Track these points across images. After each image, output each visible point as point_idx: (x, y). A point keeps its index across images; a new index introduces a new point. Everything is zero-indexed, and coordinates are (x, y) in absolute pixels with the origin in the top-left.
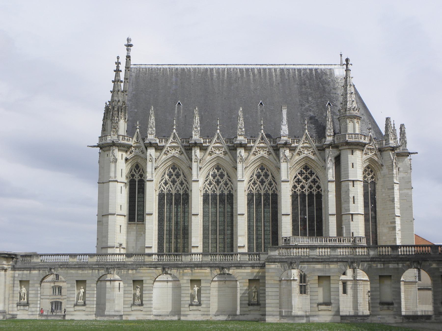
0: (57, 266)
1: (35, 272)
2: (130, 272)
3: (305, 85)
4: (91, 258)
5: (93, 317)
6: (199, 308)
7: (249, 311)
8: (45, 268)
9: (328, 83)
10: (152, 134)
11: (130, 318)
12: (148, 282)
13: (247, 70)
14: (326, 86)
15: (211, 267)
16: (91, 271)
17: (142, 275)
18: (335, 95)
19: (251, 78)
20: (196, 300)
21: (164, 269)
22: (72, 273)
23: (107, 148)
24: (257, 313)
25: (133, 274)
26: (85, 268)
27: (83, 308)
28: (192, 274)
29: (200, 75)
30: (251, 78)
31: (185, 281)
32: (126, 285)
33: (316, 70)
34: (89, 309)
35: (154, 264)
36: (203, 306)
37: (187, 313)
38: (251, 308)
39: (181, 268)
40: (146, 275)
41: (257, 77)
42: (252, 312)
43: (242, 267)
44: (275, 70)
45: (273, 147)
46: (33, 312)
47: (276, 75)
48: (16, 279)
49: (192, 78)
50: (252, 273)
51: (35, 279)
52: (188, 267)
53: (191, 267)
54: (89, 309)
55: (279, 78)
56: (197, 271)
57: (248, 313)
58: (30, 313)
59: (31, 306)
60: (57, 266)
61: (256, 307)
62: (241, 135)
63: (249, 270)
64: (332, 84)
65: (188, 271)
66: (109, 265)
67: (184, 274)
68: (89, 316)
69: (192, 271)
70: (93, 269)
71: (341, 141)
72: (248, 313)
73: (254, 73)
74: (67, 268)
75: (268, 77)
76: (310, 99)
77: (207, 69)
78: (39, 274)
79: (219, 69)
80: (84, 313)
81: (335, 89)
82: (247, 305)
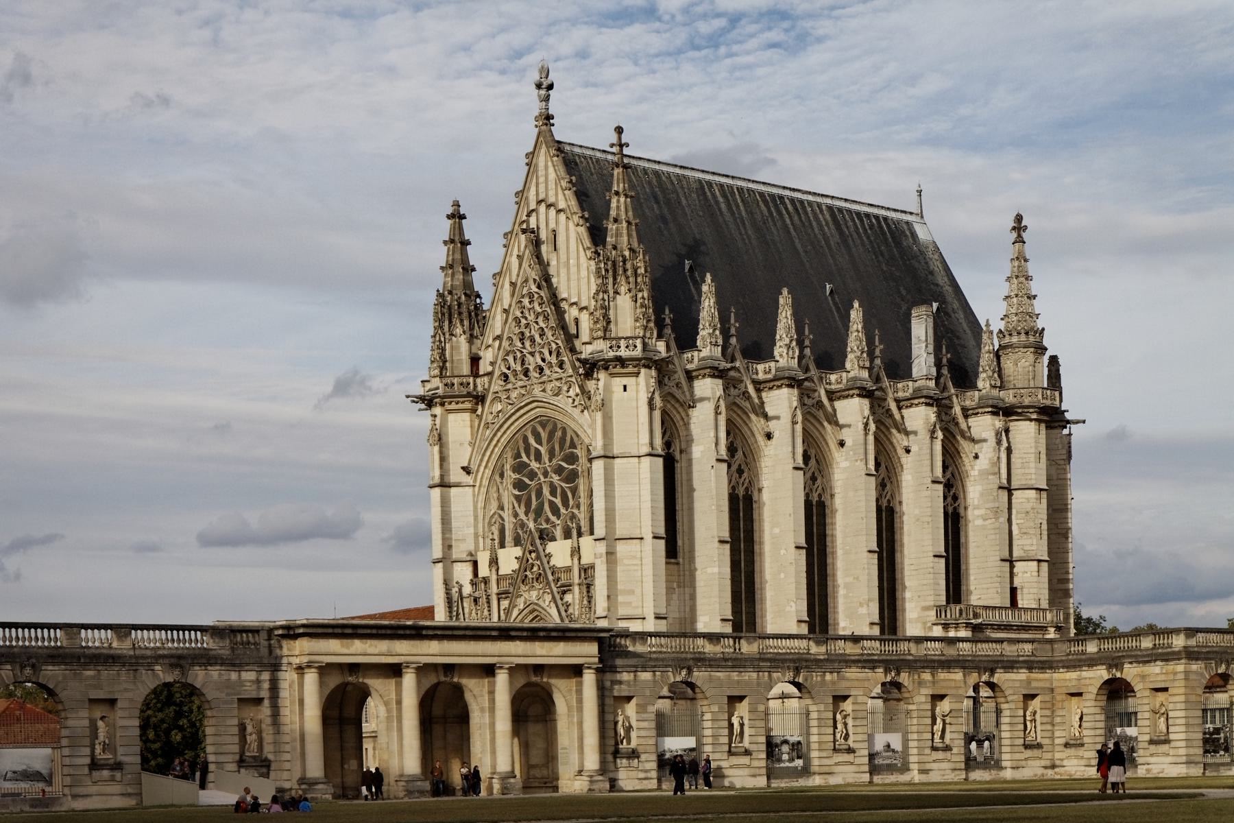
0: (691, 663)
1: (645, 676)
2: (828, 677)
3: (882, 255)
4: (749, 643)
5: (762, 782)
6: (948, 754)
7: (1026, 759)
8: (666, 666)
9: (915, 257)
10: (716, 345)
11: (834, 781)
12: (860, 699)
13: (772, 196)
14: (917, 265)
15: (964, 668)
16: (755, 675)
17: (848, 684)
18: (938, 289)
19: (788, 221)
20: (937, 737)
21: (887, 671)
22: (719, 678)
23: (630, 369)
24: (1038, 763)
25: (833, 683)
26: (744, 667)
27: (745, 760)
28: (934, 683)
29: (694, 195)
30: (788, 221)
31: (923, 699)
32: (822, 707)
33: (886, 219)
34: (756, 763)
35: (865, 661)
36: (955, 750)
37: (928, 766)
38: (1029, 753)
39: (916, 668)
40: (856, 684)
41: (796, 218)
42: (1029, 762)
43: (1012, 668)
44: (819, 205)
45: (897, 401)
46: (646, 771)
47: (827, 224)
48: (607, 693)
49: (684, 202)
50: (1029, 681)
51: (648, 693)
52: (927, 667)
53: (933, 667)
54: (756, 763)
55: (834, 231)
56: (942, 675)
57: (1023, 763)
58: (642, 775)
59: (643, 757)
60: (691, 663)
61: (1036, 752)
62: (863, 368)
63: (1022, 675)
64: (921, 258)
65: (927, 676)
66: (790, 660)
67: (921, 683)
68: (759, 778)
69: (933, 675)
70: (759, 670)
71: (1027, 401)
72: (1023, 763)
73: (786, 209)
74: (711, 666)
75: (814, 223)
76: (904, 292)
77: (700, 181)
78: (655, 681)
79: (721, 186)
80: (746, 771)
81: (932, 273)
82: (1022, 749)
